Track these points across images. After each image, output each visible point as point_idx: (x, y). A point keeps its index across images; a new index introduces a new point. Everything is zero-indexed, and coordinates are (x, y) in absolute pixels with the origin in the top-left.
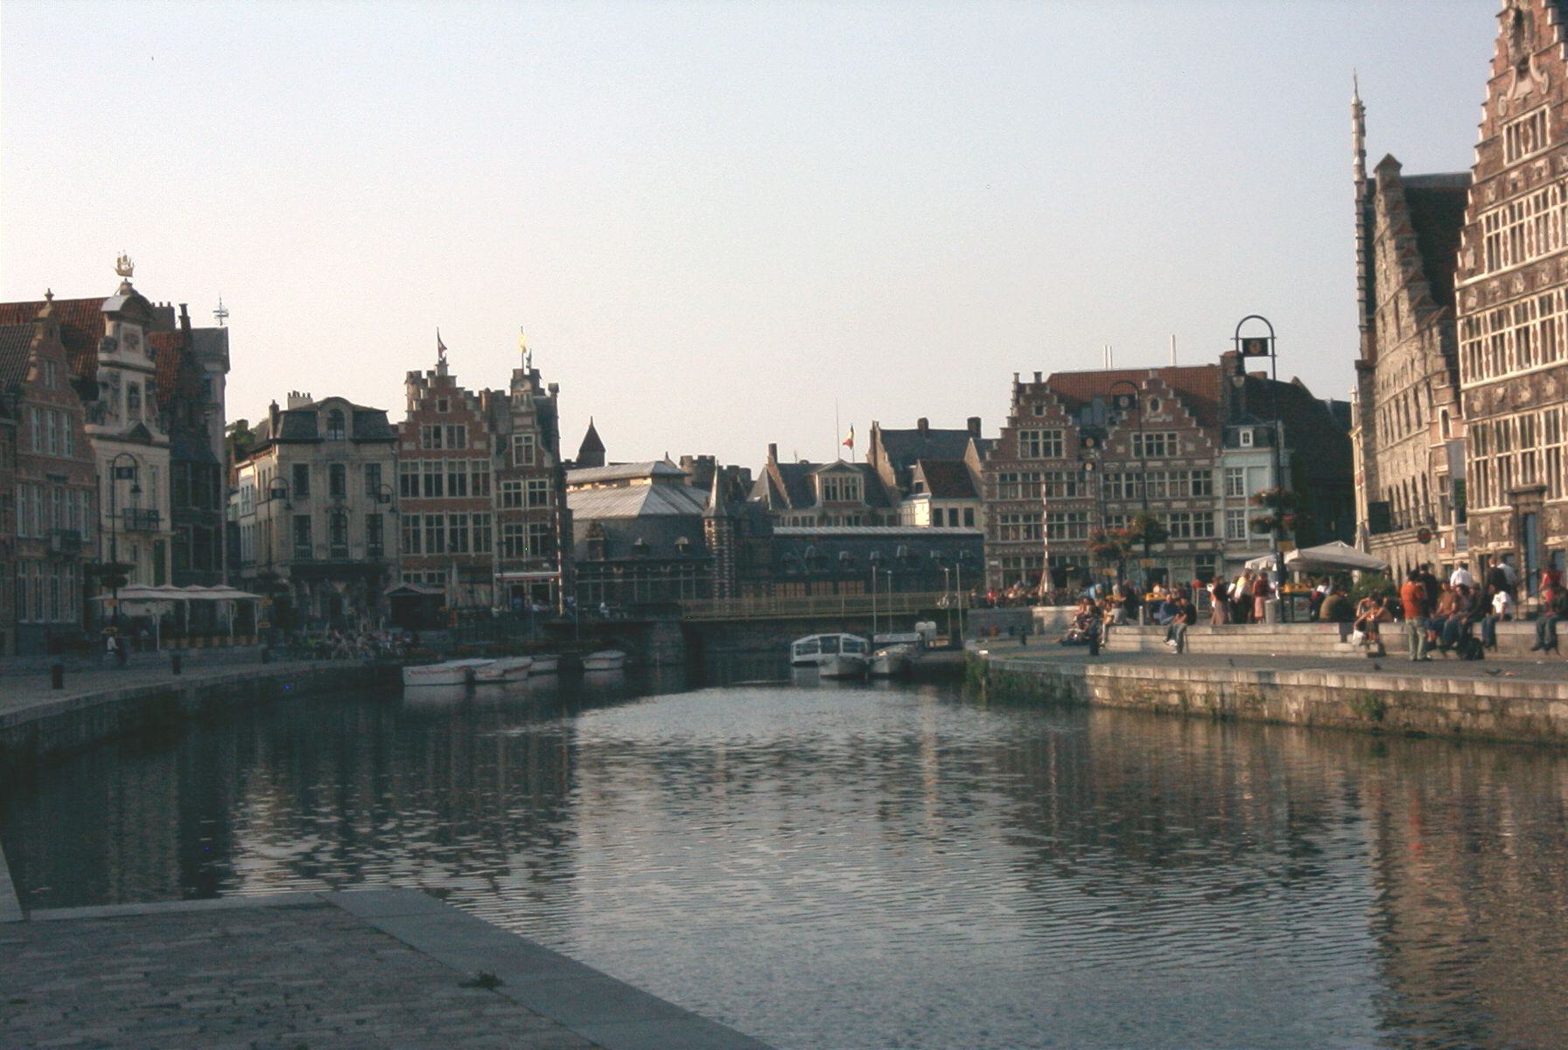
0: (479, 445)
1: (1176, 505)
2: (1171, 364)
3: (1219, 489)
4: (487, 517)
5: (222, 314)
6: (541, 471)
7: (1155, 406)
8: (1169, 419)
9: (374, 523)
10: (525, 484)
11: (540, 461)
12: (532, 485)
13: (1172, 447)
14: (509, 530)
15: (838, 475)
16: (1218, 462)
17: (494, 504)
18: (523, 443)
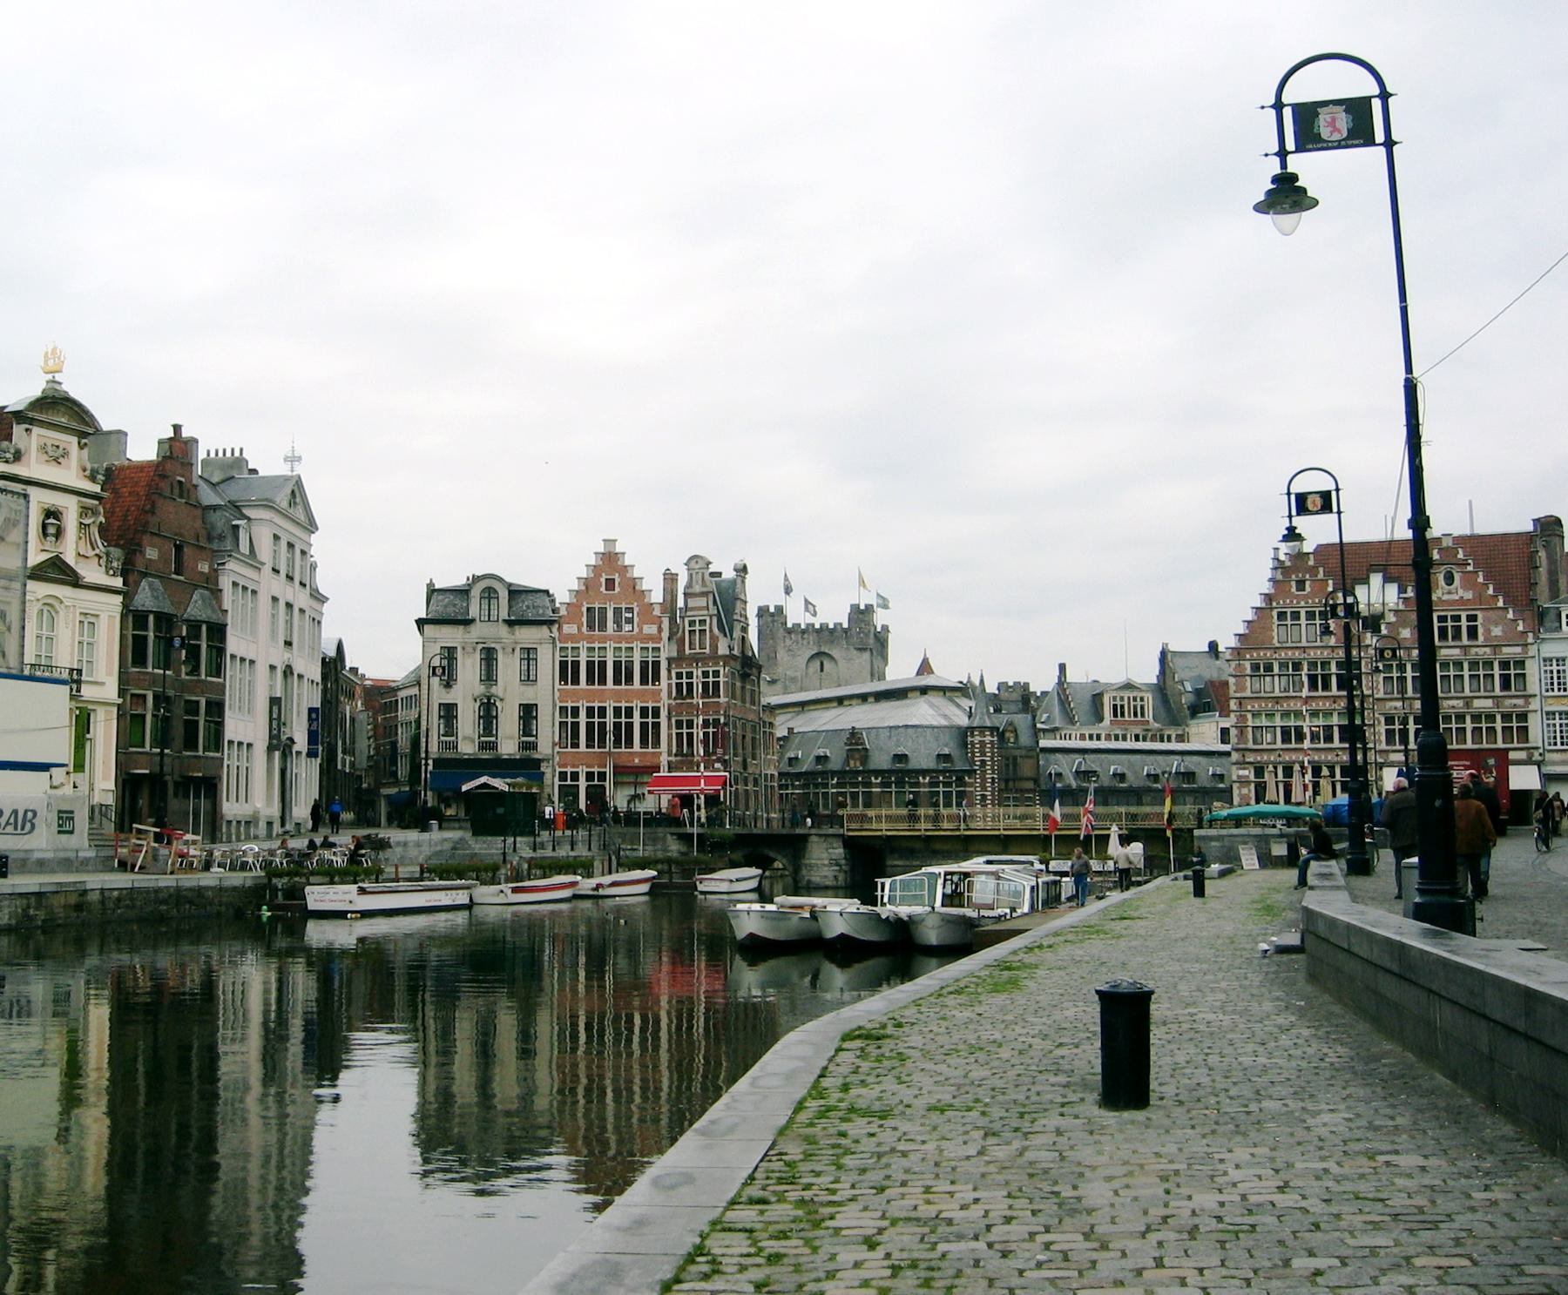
0: (651, 629)
1: (1477, 703)
2: (1468, 532)
3: (1533, 686)
4: (656, 712)
5: (293, 459)
6: (714, 657)
7: (1449, 579)
8: (1469, 595)
9: (528, 713)
10: (698, 673)
11: (714, 647)
12: (706, 674)
13: (1473, 633)
14: (679, 724)
15: (1126, 694)
16: (1532, 650)
17: (664, 694)
18: (697, 627)
